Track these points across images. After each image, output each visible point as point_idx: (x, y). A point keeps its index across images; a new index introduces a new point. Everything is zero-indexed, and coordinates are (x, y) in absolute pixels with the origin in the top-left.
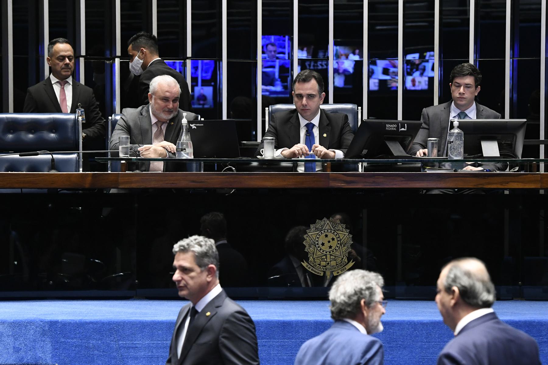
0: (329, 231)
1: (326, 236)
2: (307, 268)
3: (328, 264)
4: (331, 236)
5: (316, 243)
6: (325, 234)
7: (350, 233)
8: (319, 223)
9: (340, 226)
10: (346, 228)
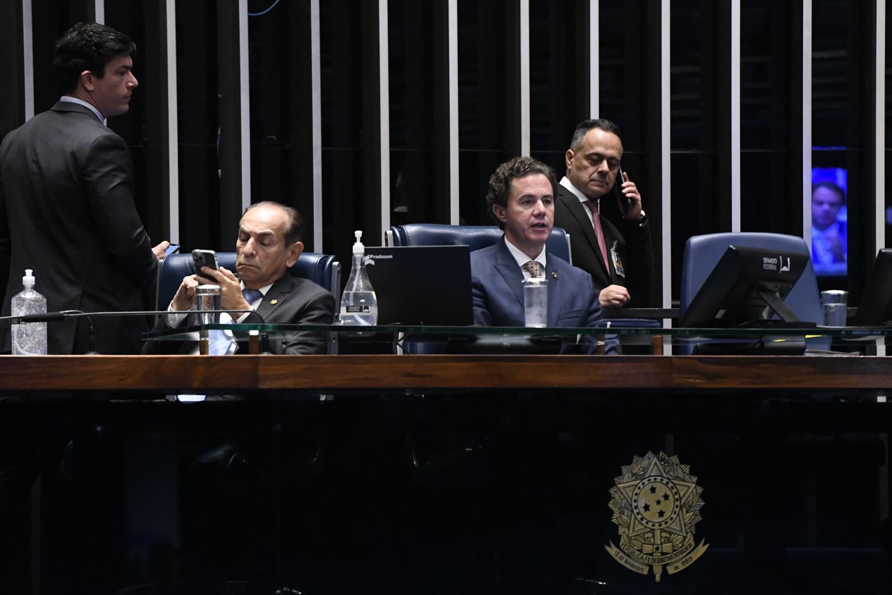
0: (659, 479)
1: (653, 490)
2: (617, 558)
3: (657, 549)
4: (662, 490)
5: (634, 504)
6: (649, 487)
7: (698, 483)
8: (639, 464)
9: (679, 470)
10: (692, 473)
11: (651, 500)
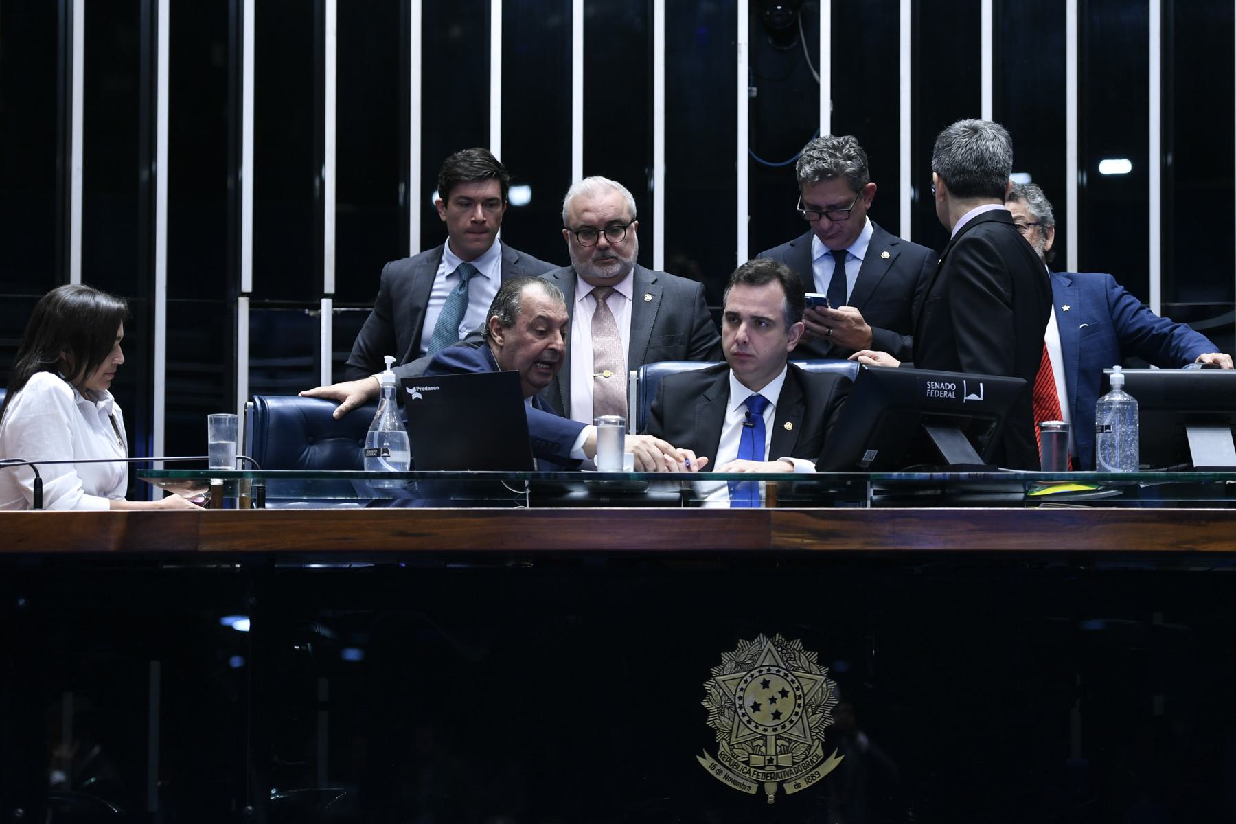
0: (774, 670)
1: (765, 684)
2: (713, 773)
3: (771, 761)
4: (777, 684)
5: (738, 703)
8: (746, 650)
9: (803, 658)
10: (821, 662)
11: (763, 697)
